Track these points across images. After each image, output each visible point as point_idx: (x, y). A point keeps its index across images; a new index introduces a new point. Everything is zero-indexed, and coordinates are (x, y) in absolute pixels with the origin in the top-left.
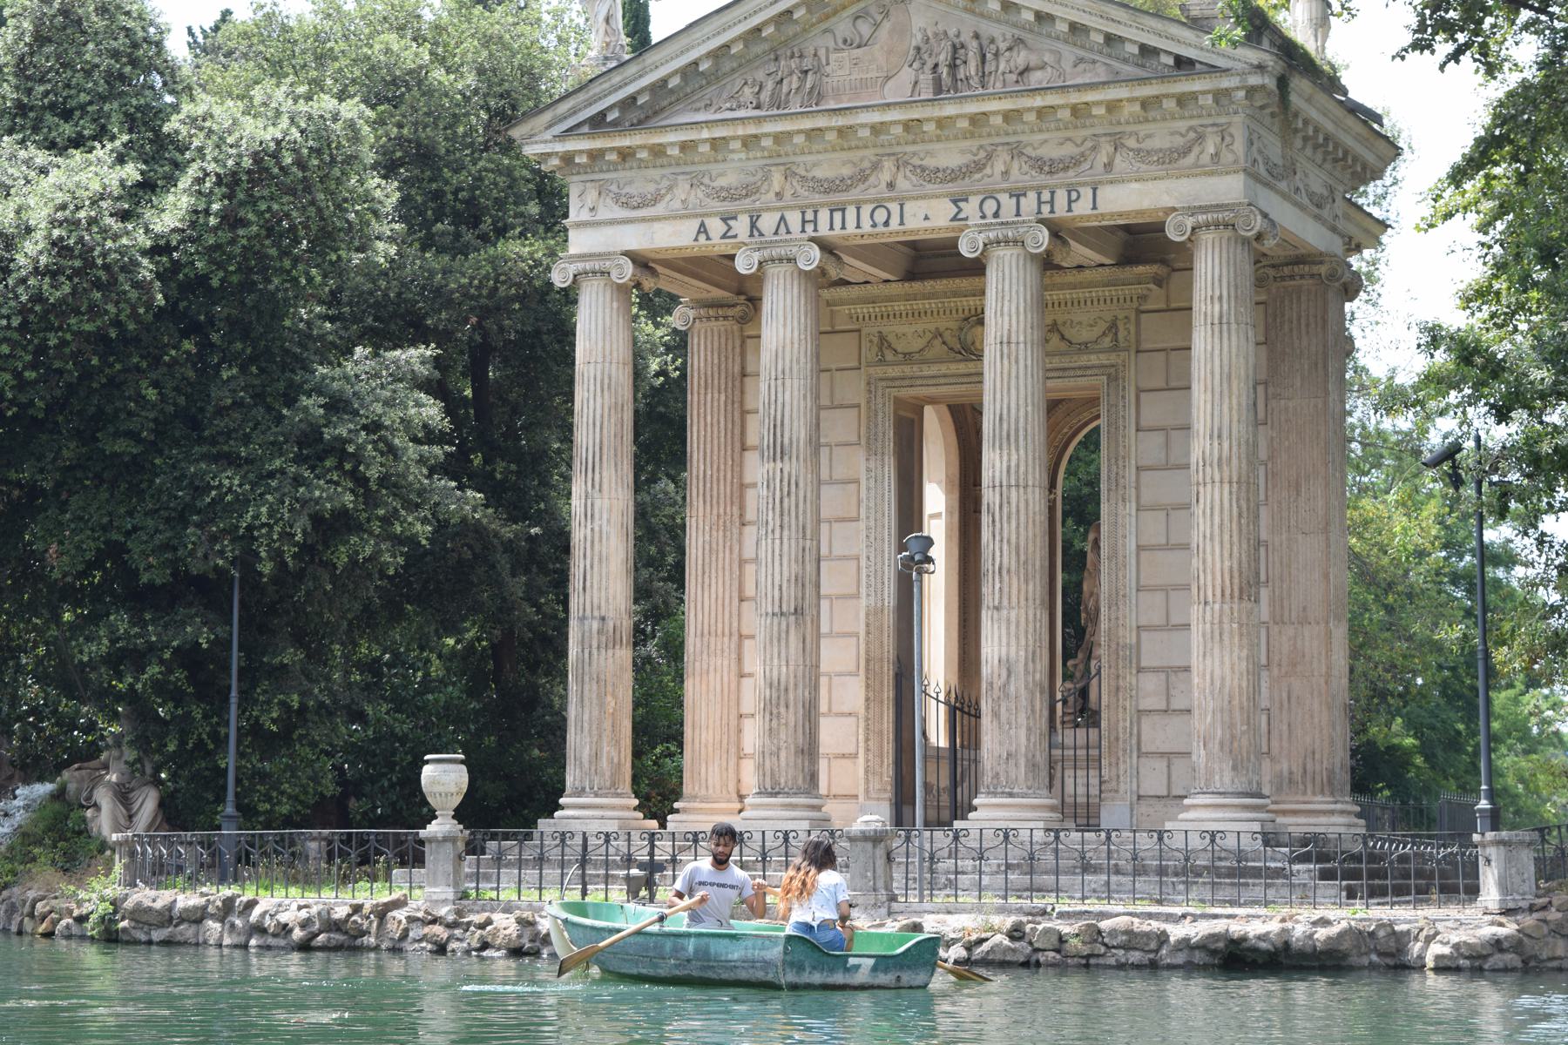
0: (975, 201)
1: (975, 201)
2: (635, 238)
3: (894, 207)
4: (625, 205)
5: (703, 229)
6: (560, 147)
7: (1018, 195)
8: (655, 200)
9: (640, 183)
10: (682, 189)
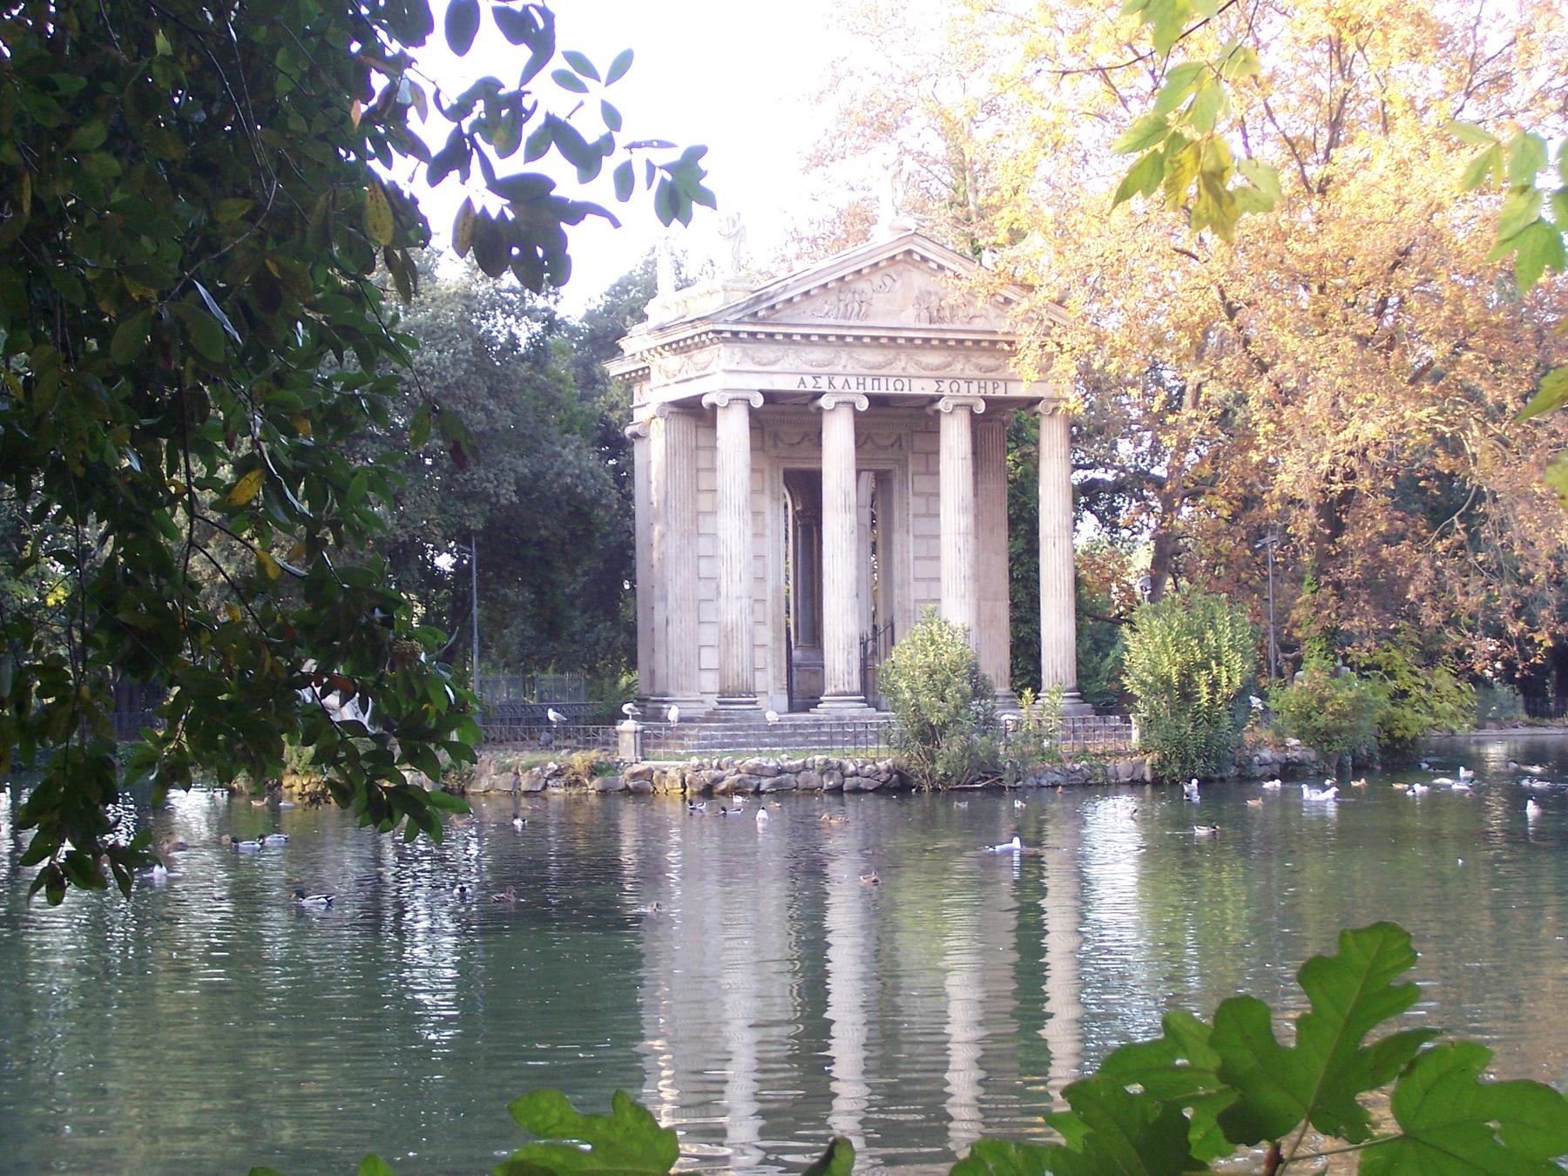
0: (948, 382)
1: (948, 382)
3: (906, 381)
4: (759, 363)
6: (735, 328)
7: (969, 381)
9: (768, 352)
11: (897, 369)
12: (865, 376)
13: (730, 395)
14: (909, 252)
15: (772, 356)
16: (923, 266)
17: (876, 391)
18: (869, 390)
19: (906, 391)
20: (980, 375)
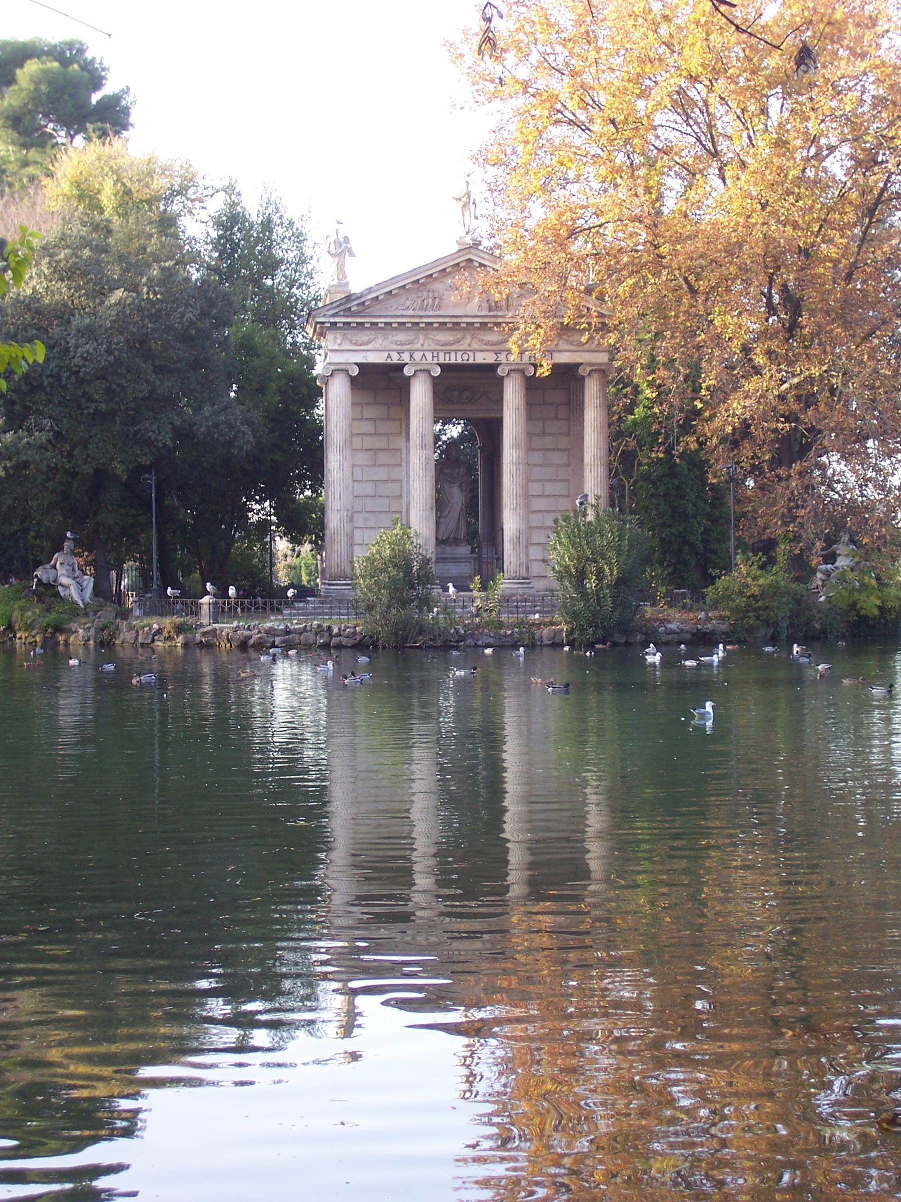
0: (504, 354)
2: (360, 358)
3: (471, 354)
4: (356, 344)
5: (389, 356)
6: (332, 320)
8: (368, 343)
9: (363, 336)
10: (379, 341)
11: (464, 345)
12: (438, 351)
13: (332, 367)
15: (366, 339)
17: (447, 361)
18: (441, 361)
19: (471, 361)
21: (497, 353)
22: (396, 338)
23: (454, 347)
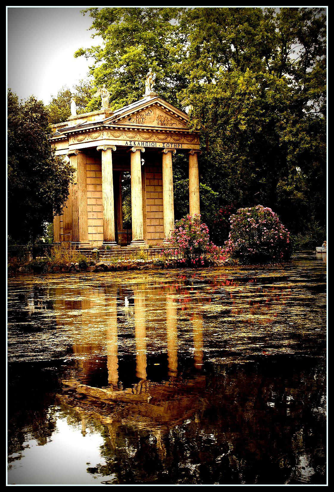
5: (127, 143)
9: (117, 134)
14: (156, 103)
16: (160, 108)
20: (175, 142)
21: (164, 143)
22: (129, 135)
23: (149, 140)
